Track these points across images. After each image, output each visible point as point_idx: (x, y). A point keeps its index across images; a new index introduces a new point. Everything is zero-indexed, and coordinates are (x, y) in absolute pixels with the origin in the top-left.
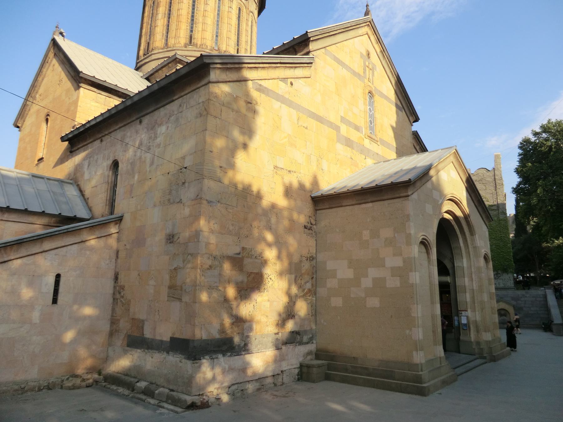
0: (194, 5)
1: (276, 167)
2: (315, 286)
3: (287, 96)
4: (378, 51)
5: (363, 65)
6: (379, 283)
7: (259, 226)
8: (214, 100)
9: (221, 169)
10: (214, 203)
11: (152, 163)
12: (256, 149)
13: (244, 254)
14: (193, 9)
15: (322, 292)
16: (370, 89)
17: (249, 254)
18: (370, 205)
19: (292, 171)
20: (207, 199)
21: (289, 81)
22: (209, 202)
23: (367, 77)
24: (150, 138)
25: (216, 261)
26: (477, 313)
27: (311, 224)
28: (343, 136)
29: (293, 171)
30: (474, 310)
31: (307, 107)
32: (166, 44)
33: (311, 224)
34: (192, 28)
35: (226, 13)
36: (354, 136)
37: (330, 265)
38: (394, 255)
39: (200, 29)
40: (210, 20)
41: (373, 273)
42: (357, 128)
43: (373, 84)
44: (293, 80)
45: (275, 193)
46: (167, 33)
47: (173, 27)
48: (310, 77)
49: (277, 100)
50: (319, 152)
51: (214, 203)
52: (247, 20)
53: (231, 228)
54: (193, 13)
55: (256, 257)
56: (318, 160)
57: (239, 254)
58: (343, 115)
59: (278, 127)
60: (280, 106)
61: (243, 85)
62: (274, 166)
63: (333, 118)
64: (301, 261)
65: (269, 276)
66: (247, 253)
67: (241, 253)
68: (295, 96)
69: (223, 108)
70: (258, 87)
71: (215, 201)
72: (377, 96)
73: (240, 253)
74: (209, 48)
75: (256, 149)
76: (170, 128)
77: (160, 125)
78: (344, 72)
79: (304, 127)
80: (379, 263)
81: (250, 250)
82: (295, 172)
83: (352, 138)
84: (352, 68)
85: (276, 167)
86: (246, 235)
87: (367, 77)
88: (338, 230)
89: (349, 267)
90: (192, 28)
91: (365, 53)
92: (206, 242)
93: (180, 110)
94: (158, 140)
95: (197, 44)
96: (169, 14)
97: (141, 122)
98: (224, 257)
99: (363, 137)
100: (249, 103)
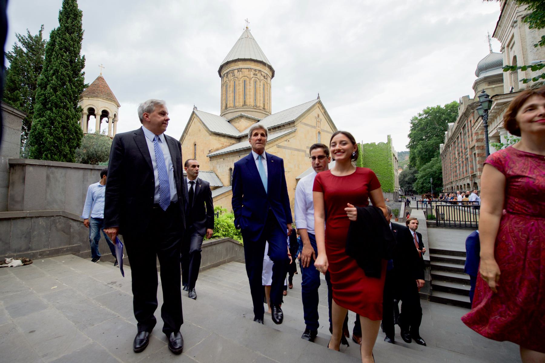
0: (245, 87)
4: (323, 112)
14: (245, 88)
16: (318, 131)
34: (245, 97)
35: (258, 88)
39: (248, 98)
40: (252, 93)
46: (234, 100)
47: (237, 97)
49: (284, 148)
54: (245, 90)
74: (252, 106)
78: (308, 128)
90: (245, 97)
91: (317, 116)
95: (247, 105)
96: (234, 91)
97: (240, 157)
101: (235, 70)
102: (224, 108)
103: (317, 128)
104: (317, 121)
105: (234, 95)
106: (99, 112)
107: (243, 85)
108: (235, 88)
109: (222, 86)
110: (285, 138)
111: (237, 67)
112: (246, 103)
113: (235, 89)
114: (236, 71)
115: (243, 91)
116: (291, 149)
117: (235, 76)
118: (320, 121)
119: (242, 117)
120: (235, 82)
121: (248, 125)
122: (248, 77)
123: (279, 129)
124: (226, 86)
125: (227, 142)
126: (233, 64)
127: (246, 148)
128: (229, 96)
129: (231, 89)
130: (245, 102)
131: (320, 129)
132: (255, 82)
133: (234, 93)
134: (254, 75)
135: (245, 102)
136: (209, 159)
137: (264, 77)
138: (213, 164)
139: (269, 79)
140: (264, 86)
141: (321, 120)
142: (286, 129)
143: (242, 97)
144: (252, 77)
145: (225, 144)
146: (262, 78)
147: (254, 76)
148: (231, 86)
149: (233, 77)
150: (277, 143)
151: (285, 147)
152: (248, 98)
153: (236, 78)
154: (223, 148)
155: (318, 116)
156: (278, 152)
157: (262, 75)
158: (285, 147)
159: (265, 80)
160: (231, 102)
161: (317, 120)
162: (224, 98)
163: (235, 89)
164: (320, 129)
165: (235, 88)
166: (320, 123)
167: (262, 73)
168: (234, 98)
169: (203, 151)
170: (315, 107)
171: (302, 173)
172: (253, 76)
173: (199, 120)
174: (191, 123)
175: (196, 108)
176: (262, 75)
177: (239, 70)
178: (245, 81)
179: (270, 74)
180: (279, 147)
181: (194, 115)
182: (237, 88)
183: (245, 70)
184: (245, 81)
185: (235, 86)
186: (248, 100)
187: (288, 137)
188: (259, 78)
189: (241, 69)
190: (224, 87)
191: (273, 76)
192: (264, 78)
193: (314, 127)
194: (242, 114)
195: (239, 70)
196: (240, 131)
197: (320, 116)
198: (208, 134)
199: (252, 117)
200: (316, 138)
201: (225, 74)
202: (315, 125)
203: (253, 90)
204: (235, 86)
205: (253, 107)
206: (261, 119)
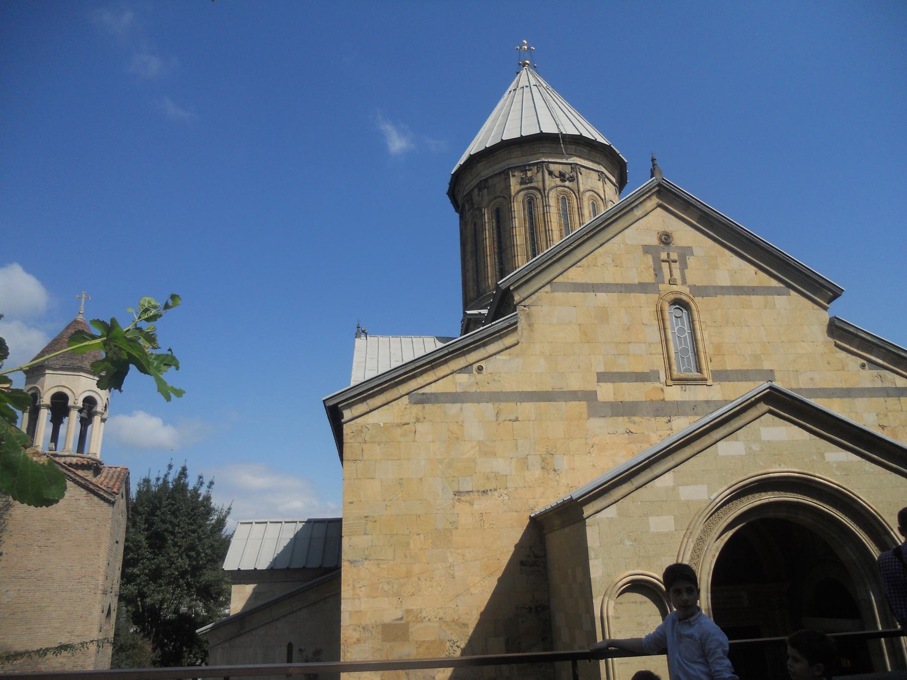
1: (457, 493)
3: (473, 389)
5: (651, 263)
7: (432, 578)
8: (351, 441)
9: (367, 519)
10: (359, 561)
12: (421, 479)
13: (410, 618)
16: (672, 297)
17: (417, 617)
19: (489, 491)
20: (350, 559)
21: (475, 366)
22: (351, 562)
23: (667, 276)
25: (366, 633)
27: (536, 556)
28: (605, 403)
29: (491, 490)
31: (515, 389)
33: (536, 556)
35: (541, 216)
43: (684, 282)
44: (482, 364)
45: (458, 528)
46: (478, 276)
48: (517, 344)
49: (454, 402)
50: (547, 446)
51: (359, 561)
52: (578, 208)
53: (386, 587)
55: (429, 619)
56: (543, 460)
57: (402, 618)
58: (601, 369)
59: (458, 439)
60: (461, 409)
61: (394, 405)
62: (454, 492)
63: (575, 383)
65: (454, 644)
66: (413, 616)
67: (405, 618)
68: (488, 383)
69: (365, 446)
71: (361, 560)
72: (697, 299)
73: (402, 618)
75: (421, 479)
78: (602, 297)
79: (510, 420)
81: (419, 611)
82: (495, 490)
83: (628, 399)
84: (621, 282)
86: (410, 593)
87: (667, 276)
91: (654, 241)
92: (350, 611)
98: (377, 626)
100: (405, 424)
101: (472, 190)
103: (661, 287)
104: (658, 262)
106: (76, 400)
107: (494, 225)
110: (461, 362)
111: (475, 182)
114: (476, 191)
116: (496, 397)
117: (476, 206)
120: (475, 225)
122: (504, 197)
131: (686, 290)
132: (530, 203)
133: (476, 256)
134: (521, 184)
137: (562, 176)
140: (564, 204)
141: (685, 252)
147: (523, 186)
149: (471, 211)
150: (413, 385)
155: (666, 239)
156: (418, 420)
157: (551, 173)
159: (567, 183)
164: (686, 290)
167: (552, 167)
168: (477, 271)
172: (518, 187)
175: (363, 332)
176: (551, 173)
180: (423, 400)
183: (496, 180)
188: (540, 185)
189: (486, 180)
192: (563, 181)
193: (643, 288)
195: (483, 185)
202: (649, 277)
203: (523, 230)
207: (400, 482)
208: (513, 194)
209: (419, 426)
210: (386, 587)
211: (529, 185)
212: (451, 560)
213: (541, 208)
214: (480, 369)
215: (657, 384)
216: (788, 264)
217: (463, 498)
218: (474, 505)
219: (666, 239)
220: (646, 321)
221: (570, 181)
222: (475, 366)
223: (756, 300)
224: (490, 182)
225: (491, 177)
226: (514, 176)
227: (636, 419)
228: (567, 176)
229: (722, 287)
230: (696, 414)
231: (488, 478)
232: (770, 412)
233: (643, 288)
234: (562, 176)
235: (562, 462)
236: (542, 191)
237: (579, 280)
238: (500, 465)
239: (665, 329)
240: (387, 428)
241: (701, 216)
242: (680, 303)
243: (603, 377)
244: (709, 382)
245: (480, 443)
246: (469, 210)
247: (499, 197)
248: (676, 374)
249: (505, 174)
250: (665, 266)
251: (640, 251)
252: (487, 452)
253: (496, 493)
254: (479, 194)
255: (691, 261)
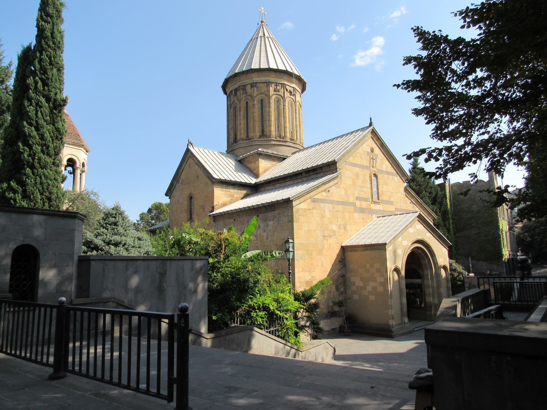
1: (324, 236)
2: (345, 289)
6: (374, 288)
11: (267, 238)
14: (262, 111)
15: (349, 292)
16: (374, 172)
18: (369, 252)
24: (265, 226)
26: (436, 299)
27: (342, 259)
30: (434, 298)
32: (248, 136)
33: (342, 259)
36: (364, 205)
37: (353, 279)
38: (381, 276)
39: (268, 125)
41: (372, 284)
42: (366, 200)
43: (376, 168)
44: (329, 189)
46: (247, 129)
53: (307, 269)
56: (344, 226)
63: (351, 200)
64: (338, 278)
69: (299, 216)
70: (313, 199)
74: (274, 136)
76: (275, 224)
77: (270, 220)
78: (357, 170)
80: (374, 280)
85: (324, 236)
88: (355, 263)
89: (361, 281)
91: (369, 150)
93: (280, 216)
94: (269, 228)
95: (267, 135)
96: (247, 116)
99: (370, 203)
101: (247, 85)
102: (231, 140)
105: (247, 121)
107: (260, 107)
108: (247, 111)
109: (229, 107)
110: (323, 188)
112: (265, 133)
113: (247, 113)
114: (249, 86)
115: (259, 115)
116: (332, 202)
117: (247, 94)
118: (376, 158)
119: (260, 154)
120: (247, 103)
121: (268, 166)
122: (266, 95)
123: (315, 172)
124: (235, 108)
125: (237, 193)
126: (243, 77)
127: (267, 205)
128: (239, 123)
129: (243, 112)
130: (263, 131)
131: (376, 171)
132: (278, 101)
133: (247, 118)
134: (275, 91)
135: (263, 131)
136: (213, 220)
137: (290, 92)
138: (219, 227)
139: (298, 95)
142: (325, 173)
143: (258, 124)
144: (273, 95)
145: (236, 196)
146: (287, 94)
148: (242, 109)
150: (311, 194)
151: (323, 201)
152: (268, 125)
153: (249, 97)
154: (231, 202)
155: (372, 150)
158: (323, 201)
159: (292, 96)
160: (243, 131)
161: (370, 157)
162: (231, 126)
163: (247, 113)
165: (247, 111)
166: (376, 161)
167: (287, 87)
168: (247, 126)
169: (203, 207)
170: (366, 138)
171: (351, 236)
173: (196, 161)
174: (184, 165)
175: (191, 144)
176: (287, 90)
177: (253, 85)
178: (262, 100)
179: (299, 89)
180: (314, 201)
181: (189, 154)
182: (250, 111)
183: (262, 85)
184: (262, 100)
185: (247, 108)
186: (268, 127)
187: (327, 186)
189: (256, 83)
190: (232, 110)
191: (303, 90)
192: (291, 95)
193: (366, 168)
194: (259, 149)
196: (256, 176)
197: (374, 149)
198: (209, 182)
199: (275, 153)
200: (371, 184)
201: (232, 91)
202: (368, 165)
204: (247, 108)
205: (276, 138)
206: (289, 155)
207: (309, 231)
208: (271, 95)
209: (314, 210)
210: (307, 269)
211: (277, 93)
212: (322, 260)
213: (282, 106)
214: (329, 191)
215: (369, 203)
216: (399, 166)
217: (325, 238)
218: (328, 241)
219: (372, 150)
220: (367, 180)
221: (293, 96)
222: (328, 190)
223: (391, 177)
224: (258, 85)
225: (259, 83)
226: (271, 86)
227: (365, 214)
228: (293, 94)
229: (384, 171)
230: (377, 214)
231: (331, 232)
232: (418, 220)
233: (366, 168)
234: (290, 92)
235: (348, 227)
236: (283, 97)
237: (353, 162)
238: (334, 227)
239: (372, 184)
240: (305, 210)
241: (381, 144)
242: (375, 175)
243: (358, 198)
244: (380, 204)
245: (329, 218)
246: (243, 94)
247: (263, 94)
248: (373, 201)
249: (268, 84)
250: (372, 160)
251: (366, 154)
252: (332, 223)
253: (333, 237)
254: (251, 88)
255: (378, 160)
